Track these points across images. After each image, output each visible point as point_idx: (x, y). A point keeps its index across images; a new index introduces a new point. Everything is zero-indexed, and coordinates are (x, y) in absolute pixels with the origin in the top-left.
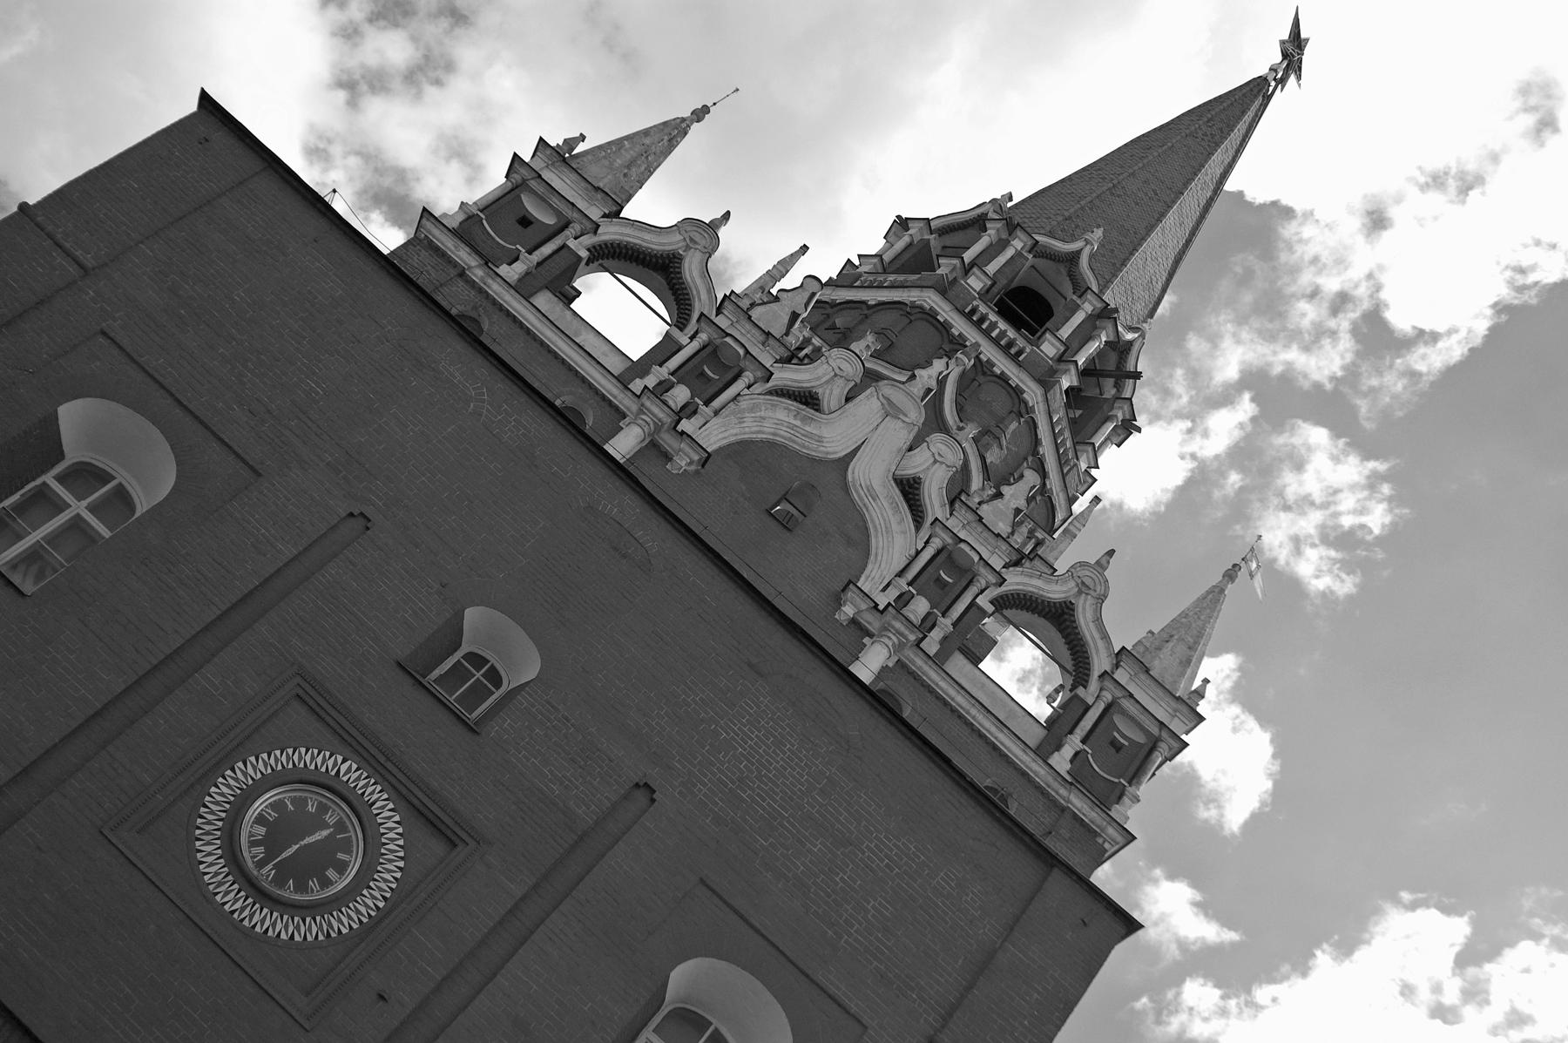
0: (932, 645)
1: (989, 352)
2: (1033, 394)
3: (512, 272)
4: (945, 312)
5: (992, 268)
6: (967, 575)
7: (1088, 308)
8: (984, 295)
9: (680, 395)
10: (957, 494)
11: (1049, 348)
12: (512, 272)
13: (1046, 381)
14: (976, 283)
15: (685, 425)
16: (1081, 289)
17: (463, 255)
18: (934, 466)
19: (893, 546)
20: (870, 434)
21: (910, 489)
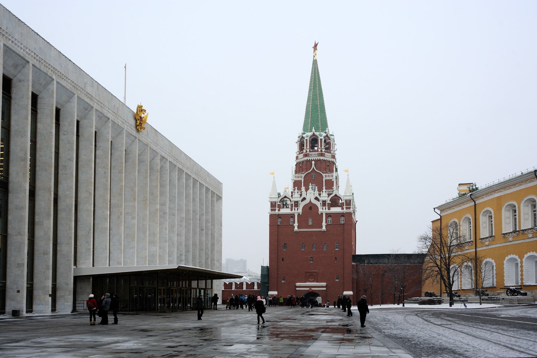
0: (327, 210)
1: (315, 158)
2: (322, 158)
3: (277, 211)
4: (308, 158)
5: (308, 147)
6: (325, 201)
7: (319, 140)
8: (310, 151)
9: (296, 208)
10: (320, 195)
11: (320, 150)
12: (277, 210)
13: (322, 155)
14: (308, 151)
15: (299, 211)
16: (317, 137)
17: (273, 212)
18: (317, 193)
19: (318, 204)
20: (311, 195)
21: (316, 199)
